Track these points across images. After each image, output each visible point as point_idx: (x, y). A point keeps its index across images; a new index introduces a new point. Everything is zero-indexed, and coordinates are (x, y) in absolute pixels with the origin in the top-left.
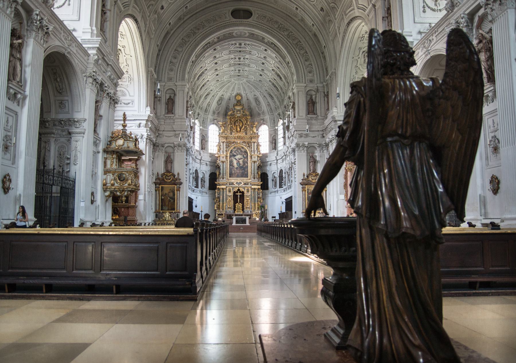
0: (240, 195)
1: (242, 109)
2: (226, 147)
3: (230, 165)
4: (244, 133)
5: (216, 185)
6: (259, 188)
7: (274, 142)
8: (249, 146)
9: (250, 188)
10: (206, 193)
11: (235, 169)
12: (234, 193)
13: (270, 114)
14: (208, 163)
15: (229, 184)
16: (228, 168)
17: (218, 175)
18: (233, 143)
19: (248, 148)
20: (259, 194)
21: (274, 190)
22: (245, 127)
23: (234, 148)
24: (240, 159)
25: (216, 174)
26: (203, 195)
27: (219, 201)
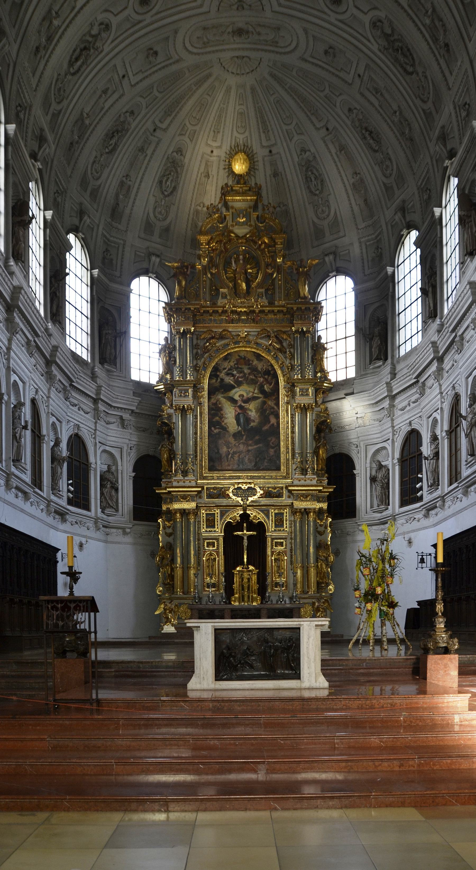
0: (249, 537)
1: (256, 202)
2: (195, 357)
3: (211, 424)
4: (264, 301)
5: (159, 499)
6: (321, 509)
7: (376, 330)
8: (282, 350)
9: (286, 512)
10: (123, 529)
11: (232, 440)
12: (229, 528)
13: (362, 225)
14: (126, 416)
15: (210, 496)
16: (207, 434)
17: (164, 462)
18: (222, 337)
19: (280, 354)
20: (321, 534)
21: (378, 515)
22: (267, 276)
23: (226, 358)
24: (247, 401)
25: (160, 461)
26: (110, 538)
27: (173, 560)
